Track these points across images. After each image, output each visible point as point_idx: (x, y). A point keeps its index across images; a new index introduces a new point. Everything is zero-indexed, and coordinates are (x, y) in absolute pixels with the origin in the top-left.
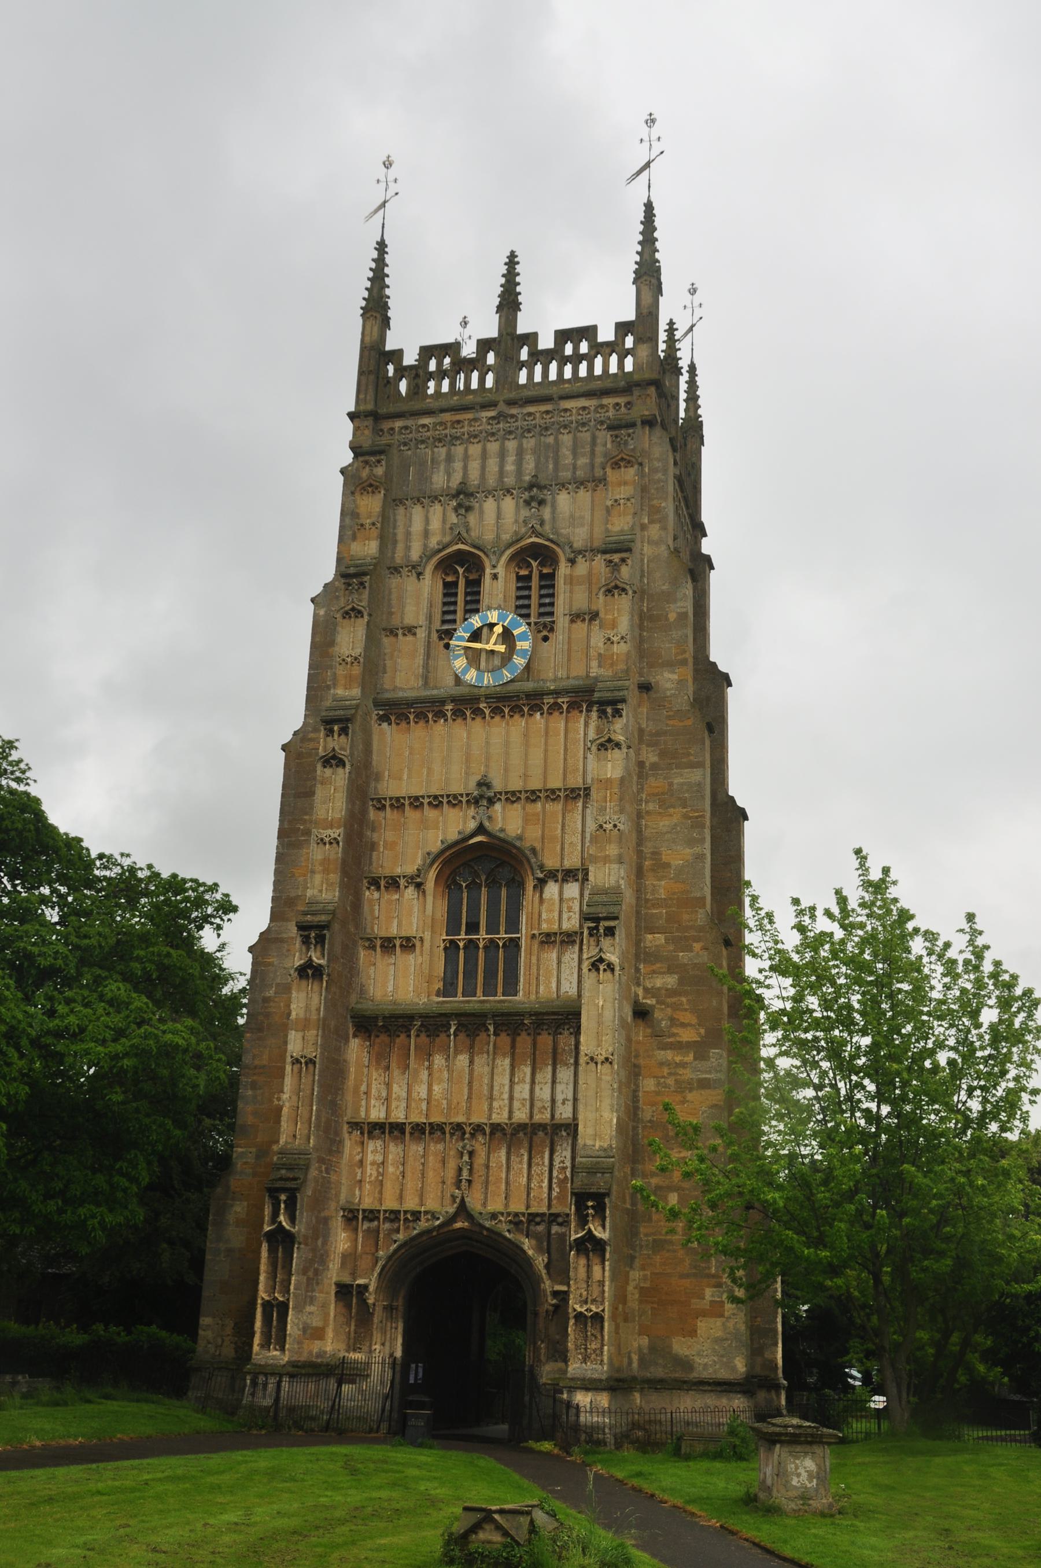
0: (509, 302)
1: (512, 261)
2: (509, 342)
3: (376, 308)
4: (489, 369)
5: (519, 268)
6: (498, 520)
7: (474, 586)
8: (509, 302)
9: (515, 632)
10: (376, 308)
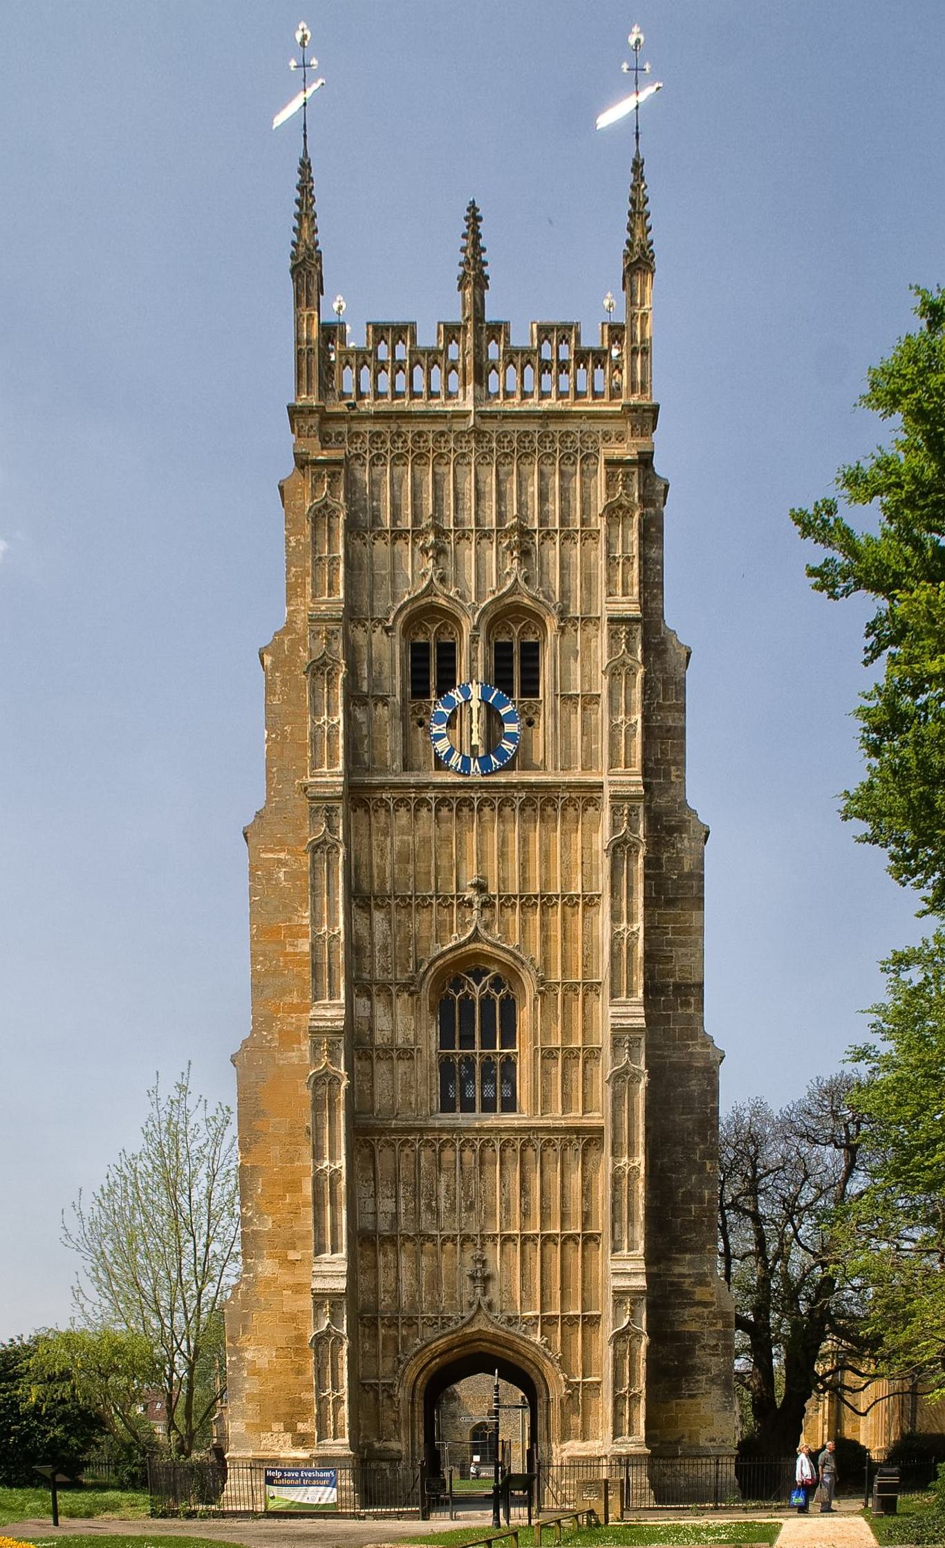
0: (475, 277)
1: (474, 218)
5: (483, 228)
6: (481, 577)
8: (475, 277)
9: (503, 712)
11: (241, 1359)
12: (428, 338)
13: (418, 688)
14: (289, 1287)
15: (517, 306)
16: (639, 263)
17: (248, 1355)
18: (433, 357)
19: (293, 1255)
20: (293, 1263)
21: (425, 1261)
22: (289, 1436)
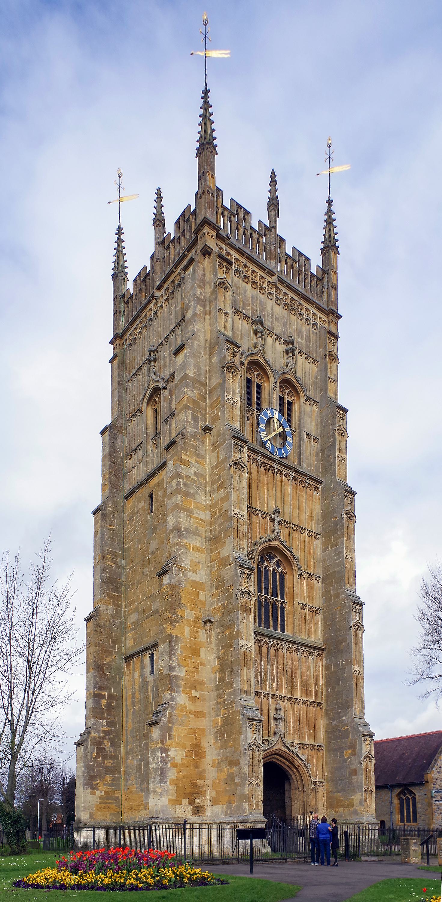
11: (167, 756)
14: (192, 713)
17: (171, 753)
19: (195, 694)
20: (195, 698)
22: (190, 807)
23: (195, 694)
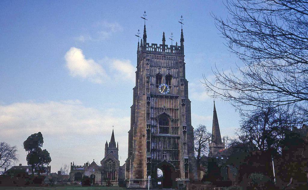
0: (164, 40)
1: (164, 34)
2: (164, 45)
3: (145, 37)
4: (161, 49)
7: (161, 79)
8: (164, 40)
10: (145, 37)
12: (158, 46)
13: (157, 83)
15: (168, 43)
16: (182, 40)
18: (159, 48)
21: (158, 153)
23: (140, 151)
